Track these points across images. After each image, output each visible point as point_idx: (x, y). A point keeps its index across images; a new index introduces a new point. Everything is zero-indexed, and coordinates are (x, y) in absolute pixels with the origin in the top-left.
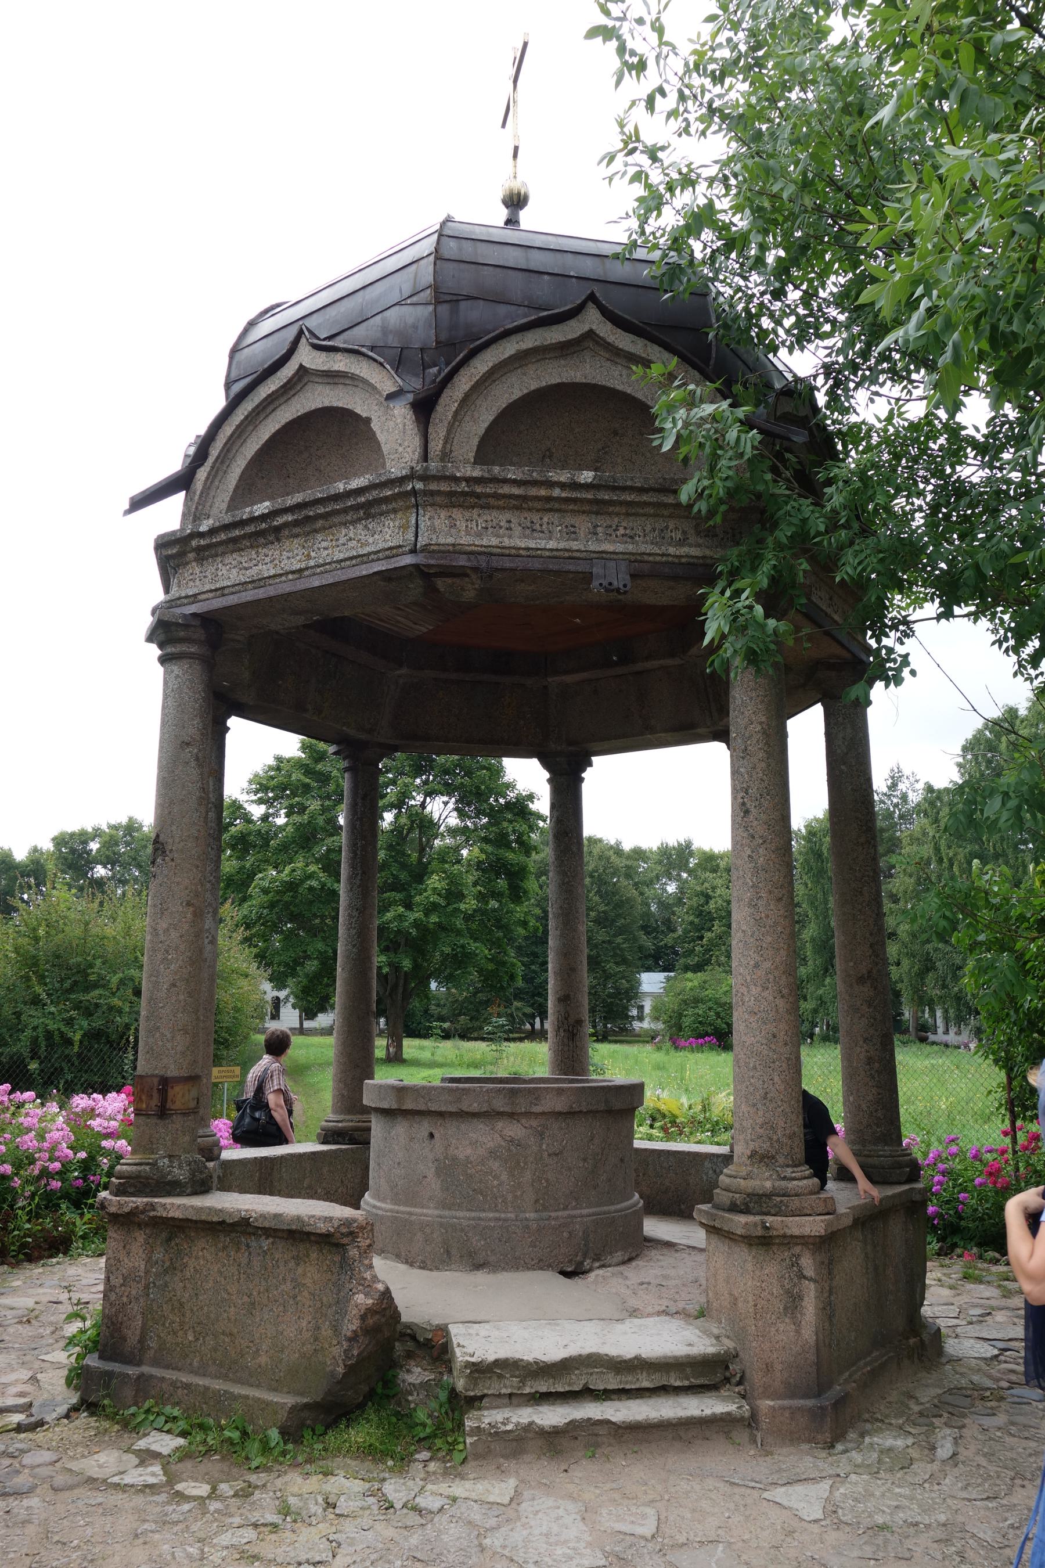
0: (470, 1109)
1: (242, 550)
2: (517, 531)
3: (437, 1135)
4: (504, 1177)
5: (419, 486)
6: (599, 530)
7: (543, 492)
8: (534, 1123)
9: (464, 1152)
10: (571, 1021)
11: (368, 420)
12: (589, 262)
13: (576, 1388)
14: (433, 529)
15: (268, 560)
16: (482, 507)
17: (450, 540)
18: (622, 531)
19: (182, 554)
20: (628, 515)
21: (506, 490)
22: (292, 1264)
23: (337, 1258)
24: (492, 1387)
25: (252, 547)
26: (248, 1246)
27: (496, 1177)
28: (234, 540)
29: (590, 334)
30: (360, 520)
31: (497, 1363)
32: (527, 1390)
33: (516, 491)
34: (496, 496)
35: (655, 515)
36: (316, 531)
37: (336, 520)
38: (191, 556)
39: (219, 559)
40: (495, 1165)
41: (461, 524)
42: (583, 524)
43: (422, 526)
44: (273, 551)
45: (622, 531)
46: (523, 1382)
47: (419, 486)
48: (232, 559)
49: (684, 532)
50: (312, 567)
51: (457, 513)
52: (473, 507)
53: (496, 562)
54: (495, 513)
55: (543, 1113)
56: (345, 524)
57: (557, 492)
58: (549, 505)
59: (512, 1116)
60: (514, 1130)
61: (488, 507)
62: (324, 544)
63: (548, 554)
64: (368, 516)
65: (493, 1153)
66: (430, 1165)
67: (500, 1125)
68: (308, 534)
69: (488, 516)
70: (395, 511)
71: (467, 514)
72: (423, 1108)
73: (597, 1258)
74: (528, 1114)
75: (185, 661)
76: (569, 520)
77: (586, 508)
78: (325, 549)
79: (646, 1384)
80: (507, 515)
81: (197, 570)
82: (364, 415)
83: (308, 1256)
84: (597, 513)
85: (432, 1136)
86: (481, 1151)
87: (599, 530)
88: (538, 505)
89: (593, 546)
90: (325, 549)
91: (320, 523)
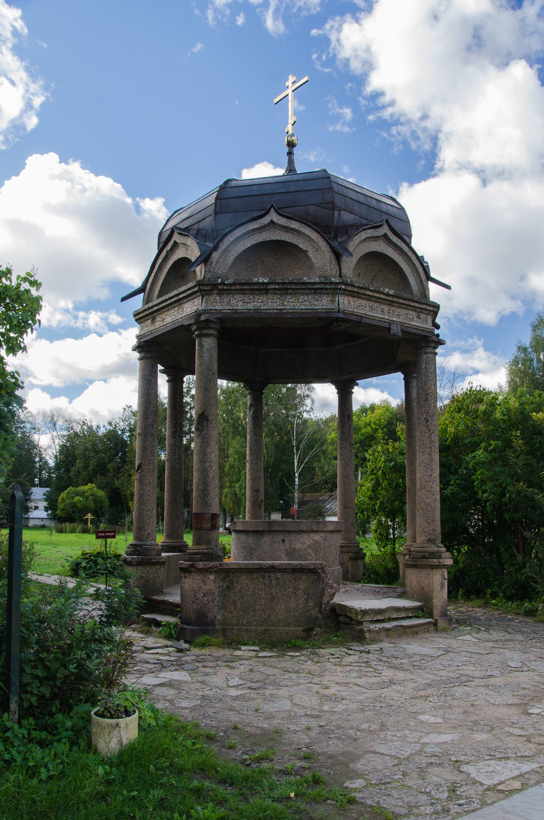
0: (303, 529)
1: (245, 294)
2: (368, 309)
3: (286, 540)
4: (313, 555)
5: (343, 287)
6: (390, 311)
7: (378, 295)
8: (323, 535)
9: (298, 546)
11: (306, 251)
12: (374, 202)
15: (260, 301)
16: (358, 297)
17: (351, 310)
18: (396, 313)
20: (398, 307)
21: (368, 293)
22: (293, 581)
23: (315, 577)
25: (251, 294)
26: (269, 577)
27: (311, 555)
29: (385, 235)
30: (310, 294)
31: (370, 610)
32: (375, 619)
33: (371, 294)
34: (364, 294)
35: (406, 309)
36: (287, 294)
37: (299, 291)
39: (231, 296)
40: (310, 551)
41: (352, 303)
42: (386, 308)
44: (264, 298)
47: (343, 287)
48: (239, 297)
50: (287, 309)
51: (350, 298)
52: (355, 297)
53: (364, 320)
54: (361, 300)
55: (327, 531)
56: (302, 294)
57: (382, 296)
58: (378, 300)
59: (316, 532)
60: (317, 537)
61: (360, 298)
62: (291, 300)
63: (378, 319)
66: (283, 552)
67: (312, 535)
68: (283, 294)
70: (328, 294)
71: (354, 300)
72: (282, 529)
74: (321, 532)
75: (212, 337)
76: (383, 306)
77: (388, 303)
78: (292, 302)
79: (403, 616)
81: (218, 298)
82: (304, 249)
83: (301, 578)
84: (390, 305)
85: (283, 541)
86: (305, 546)
87: (390, 311)
88: (374, 299)
90: (292, 302)
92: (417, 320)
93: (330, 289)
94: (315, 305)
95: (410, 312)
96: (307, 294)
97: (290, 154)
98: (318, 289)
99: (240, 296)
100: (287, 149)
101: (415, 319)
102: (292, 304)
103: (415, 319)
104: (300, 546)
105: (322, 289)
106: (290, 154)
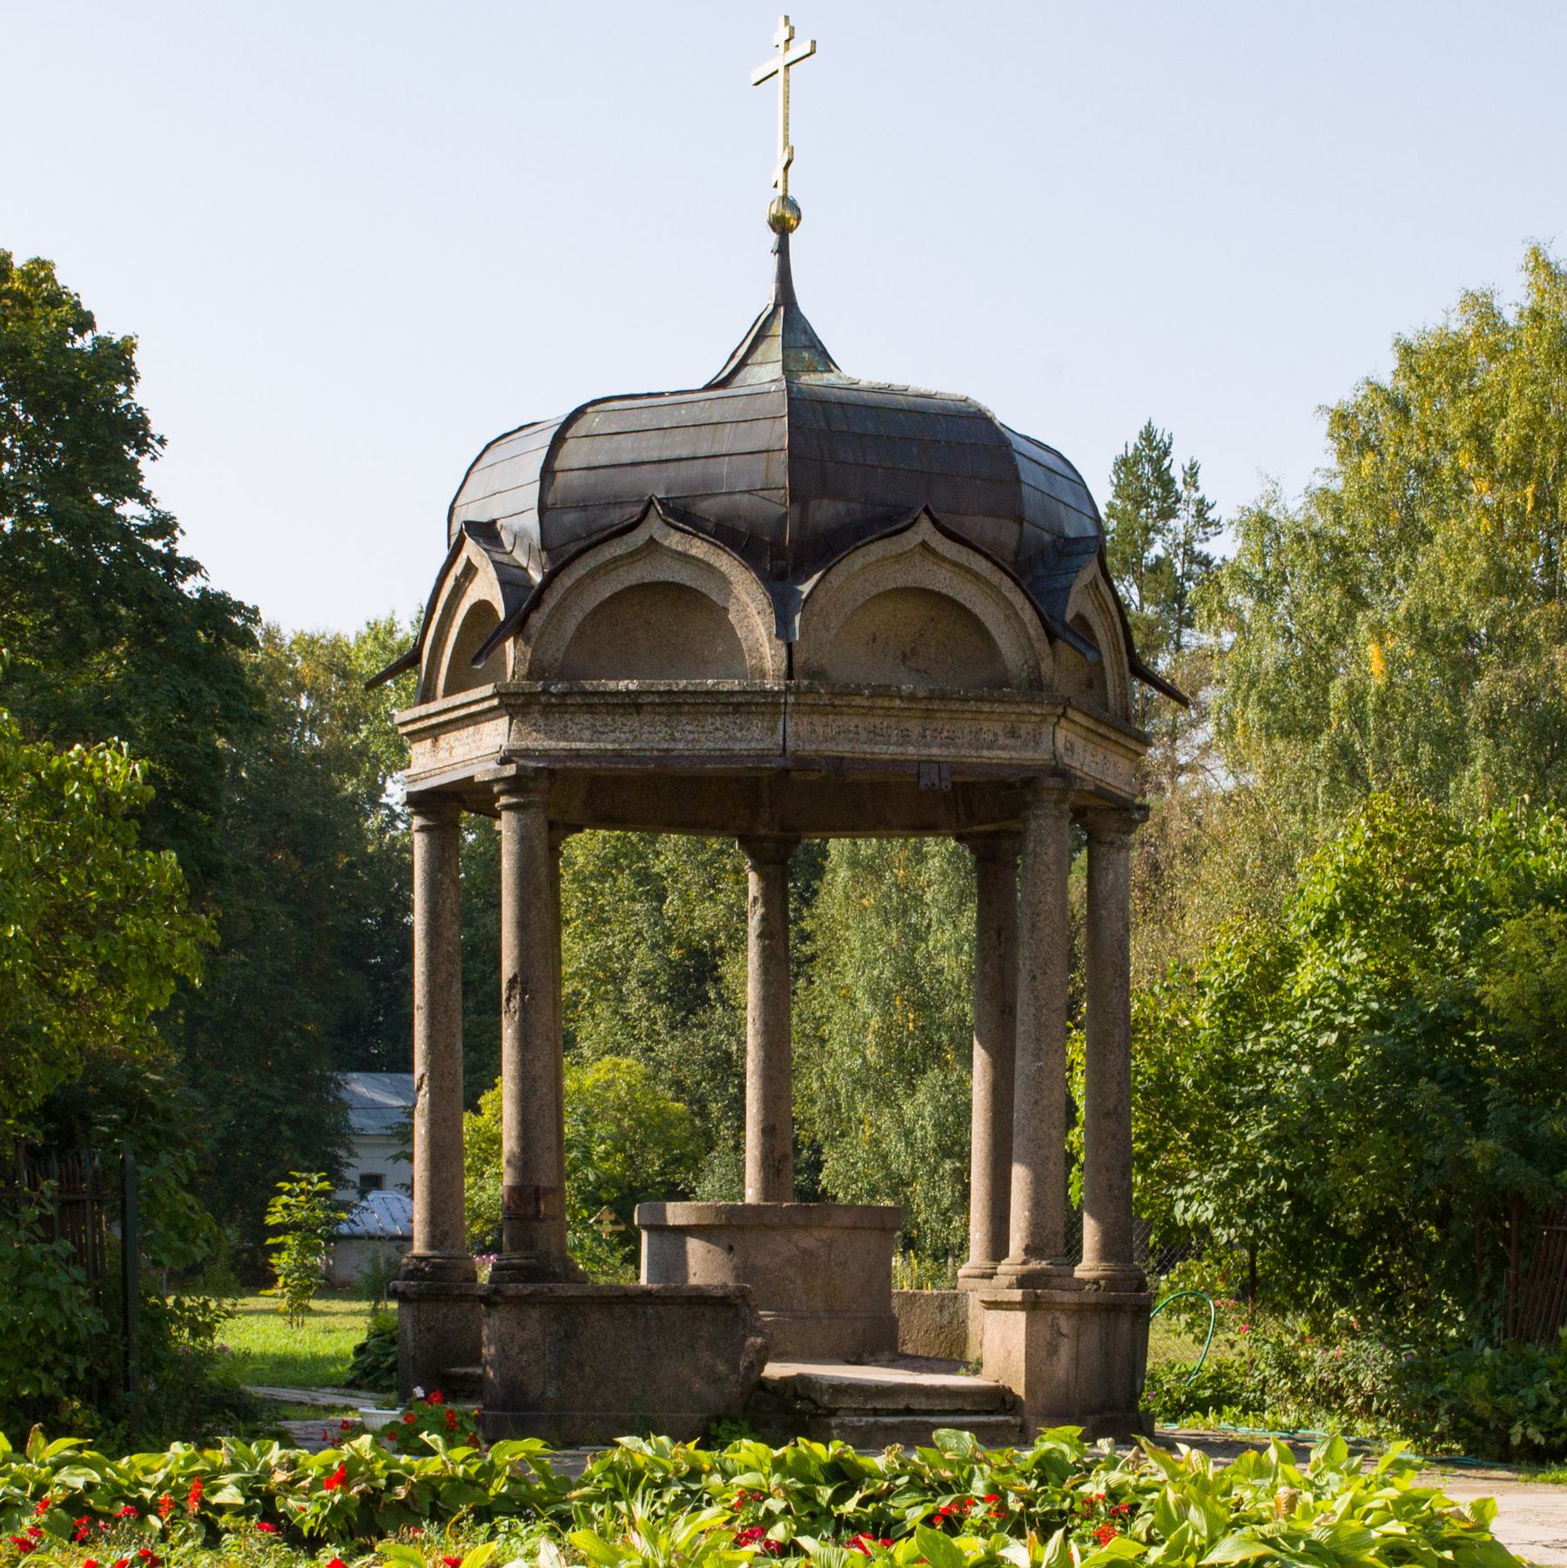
2: (863, 736)
4: (799, 1281)
10: (777, 1155)
13: (901, 1406)
14: (797, 735)
18: (945, 734)
19: (526, 705)
24: (846, 1402)
28: (590, 705)
30: (727, 714)
33: (866, 703)
38: (536, 708)
39: (568, 717)
41: (820, 730)
43: (789, 730)
45: (945, 734)
46: (866, 1401)
49: (996, 735)
54: (846, 719)
60: (807, 1241)
62: (689, 728)
64: (736, 712)
65: (789, 1261)
69: (843, 721)
70: (763, 713)
73: (872, 1354)
80: (856, 720)
89: (925, 751)
91: (686, 708)
92: (1008, 742)
93: (765, 704)
94: (736, 739)
95: (985, 726)
96: (721, 714)
97: (783, 251)
98: (740, 704)
99: (587, 717)
100: (773, 238)
101: (1001, 740)
102: (691, 737)
103: (1001, 740)
104: (768, 1260)
105: (749, 704)
106: (783, 251)
